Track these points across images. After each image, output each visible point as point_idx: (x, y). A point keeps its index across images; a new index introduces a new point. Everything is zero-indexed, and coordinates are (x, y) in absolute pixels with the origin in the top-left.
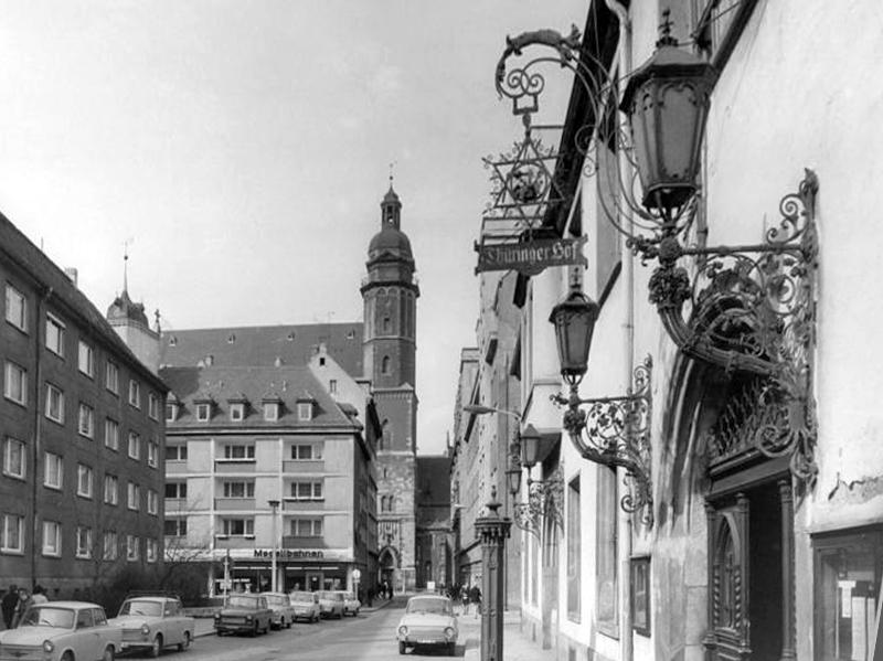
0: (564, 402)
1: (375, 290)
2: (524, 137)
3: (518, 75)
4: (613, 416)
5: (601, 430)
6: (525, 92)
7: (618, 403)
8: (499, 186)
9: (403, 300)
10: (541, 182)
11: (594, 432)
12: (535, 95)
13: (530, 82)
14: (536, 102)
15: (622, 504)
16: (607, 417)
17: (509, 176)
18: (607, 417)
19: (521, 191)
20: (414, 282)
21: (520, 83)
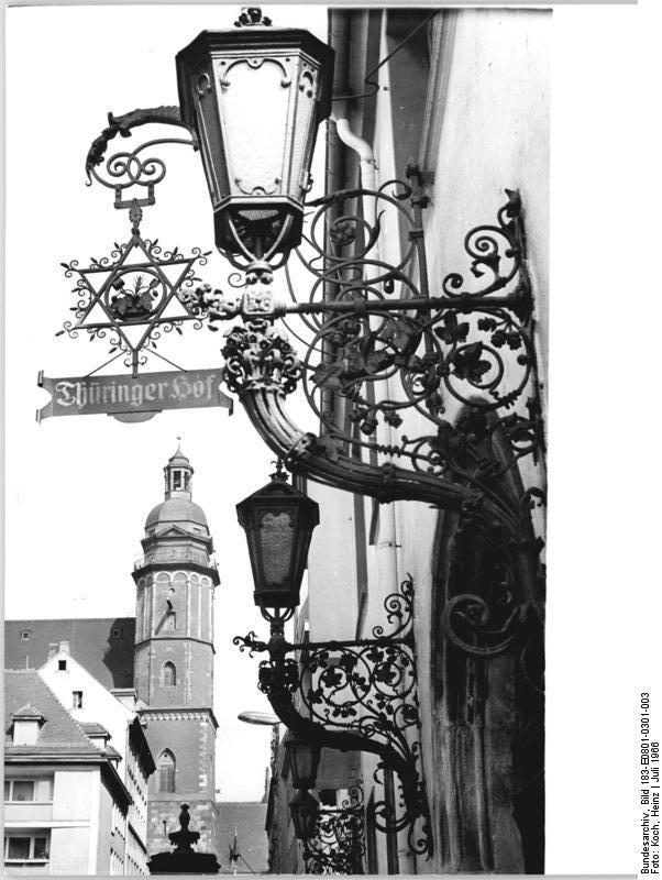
3: (125, 160)
4: (349, 670)
5: (327, 692)
6: (135, 181)
7: (357, 650)
10: (156, 294)
12: (151, 185)
13: (142, 170)
14: (151, 193)
17: (105, 289)
18: (337, 671)
19: (122, 310)
21: (127, 169)
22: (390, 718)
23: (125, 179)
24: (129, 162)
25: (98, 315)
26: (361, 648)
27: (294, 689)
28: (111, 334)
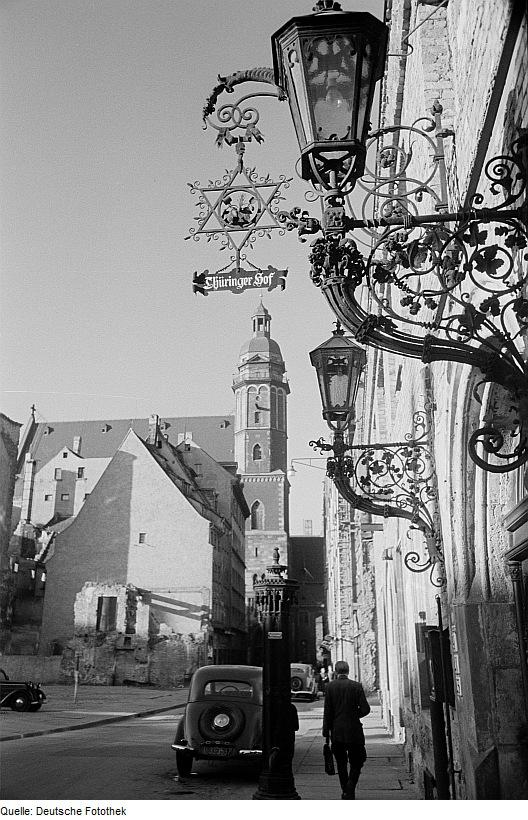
0: (328, 448)
1: (245, 388)
2: (237, 164)
3: (230, 109)
4: (388, 463)
5: (373, 478)
7: (395, 449)
8: (206, 210)
9: (273, 397)
11: (366, 481)
15: (406, 562)
16: (380, 464)
18: (380, 464)
20: (284, 381)
22: (417, 495)
23: (230, 124)
24: (233, 111)
25: (214, 223)
26: (397, 448)
27: (351, 476)
28: (222, 237)
